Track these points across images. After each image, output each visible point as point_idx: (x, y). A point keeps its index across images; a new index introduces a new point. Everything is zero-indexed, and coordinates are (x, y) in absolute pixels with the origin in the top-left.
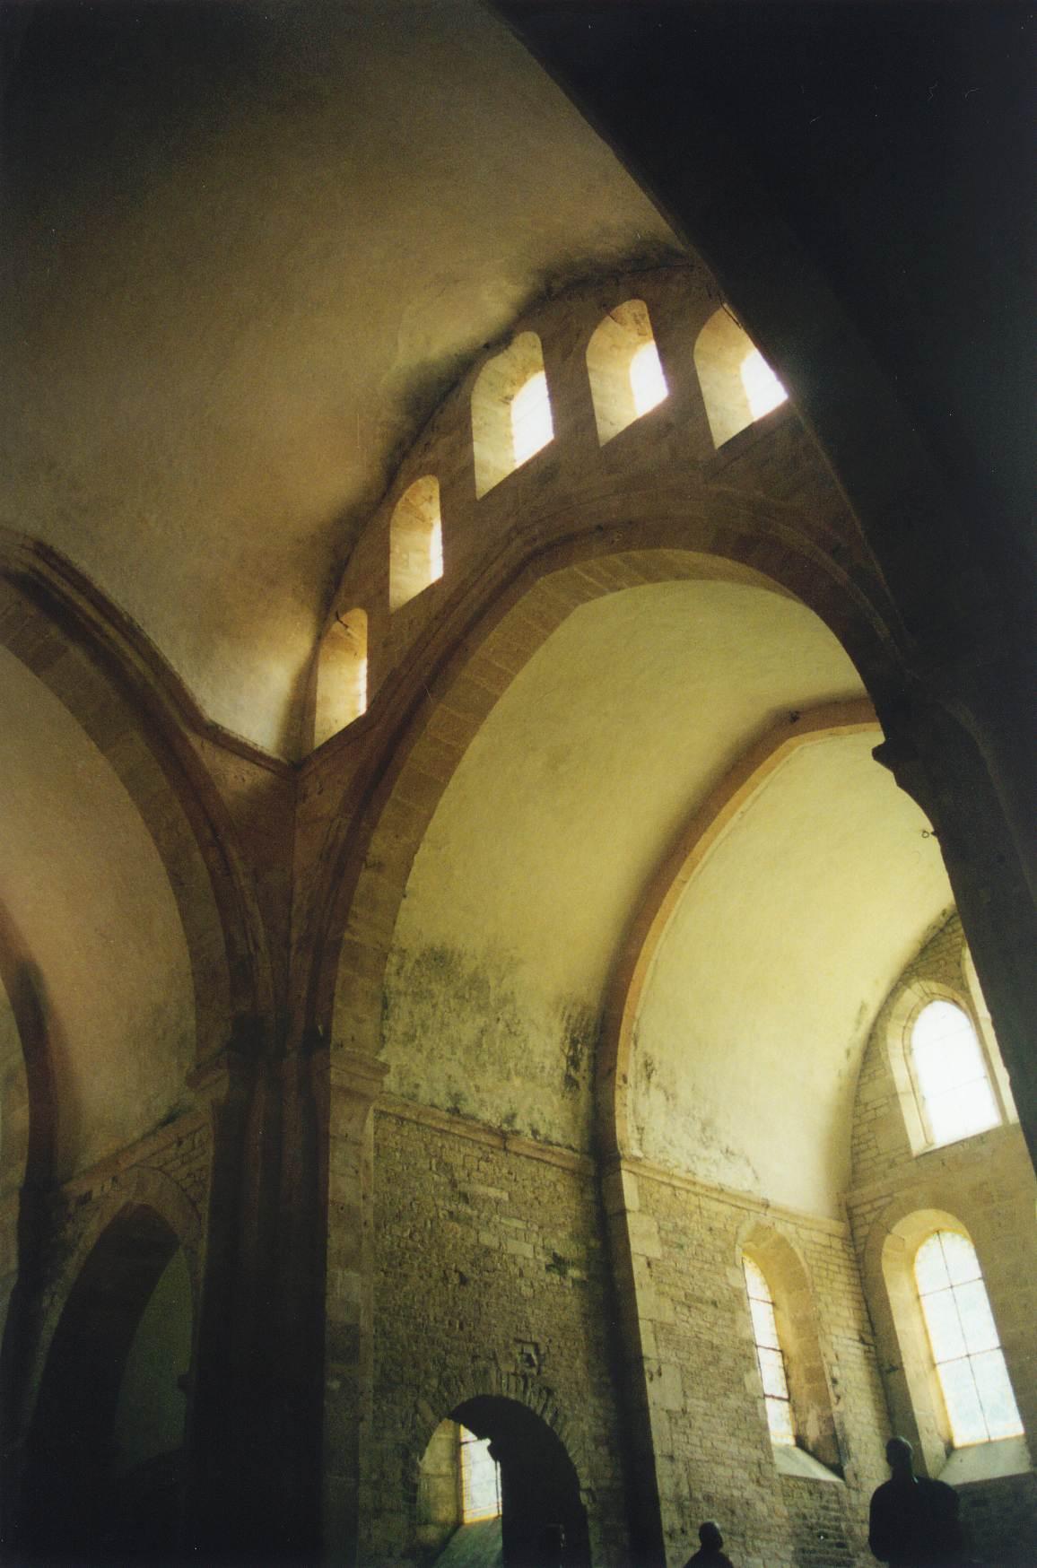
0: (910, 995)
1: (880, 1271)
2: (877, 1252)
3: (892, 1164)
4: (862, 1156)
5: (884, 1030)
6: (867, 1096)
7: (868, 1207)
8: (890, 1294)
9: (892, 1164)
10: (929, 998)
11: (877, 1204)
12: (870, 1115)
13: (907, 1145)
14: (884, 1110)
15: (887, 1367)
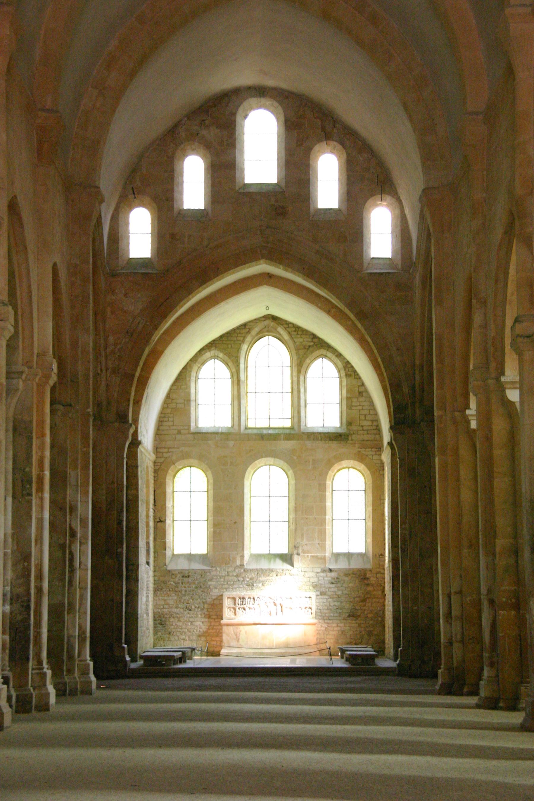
0: (208, 354)
1: (165, 479)
2: (166, 472)
3: (179, 432)
4: (164, 424)
5: (191, 367)
6: (174, 396)
7: (166, 450)
8: (167, 490)
9: (179, 432)
10: (215, 357)
11: (170, 450)
12: (173, 405)
13: (189, 426)
14: (182, 406)
15: (158, 520)
